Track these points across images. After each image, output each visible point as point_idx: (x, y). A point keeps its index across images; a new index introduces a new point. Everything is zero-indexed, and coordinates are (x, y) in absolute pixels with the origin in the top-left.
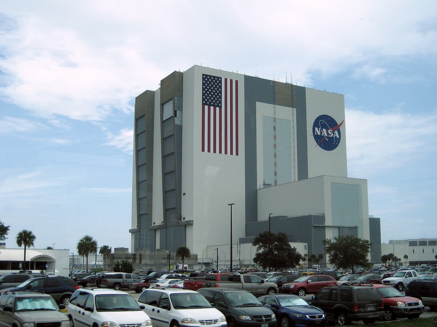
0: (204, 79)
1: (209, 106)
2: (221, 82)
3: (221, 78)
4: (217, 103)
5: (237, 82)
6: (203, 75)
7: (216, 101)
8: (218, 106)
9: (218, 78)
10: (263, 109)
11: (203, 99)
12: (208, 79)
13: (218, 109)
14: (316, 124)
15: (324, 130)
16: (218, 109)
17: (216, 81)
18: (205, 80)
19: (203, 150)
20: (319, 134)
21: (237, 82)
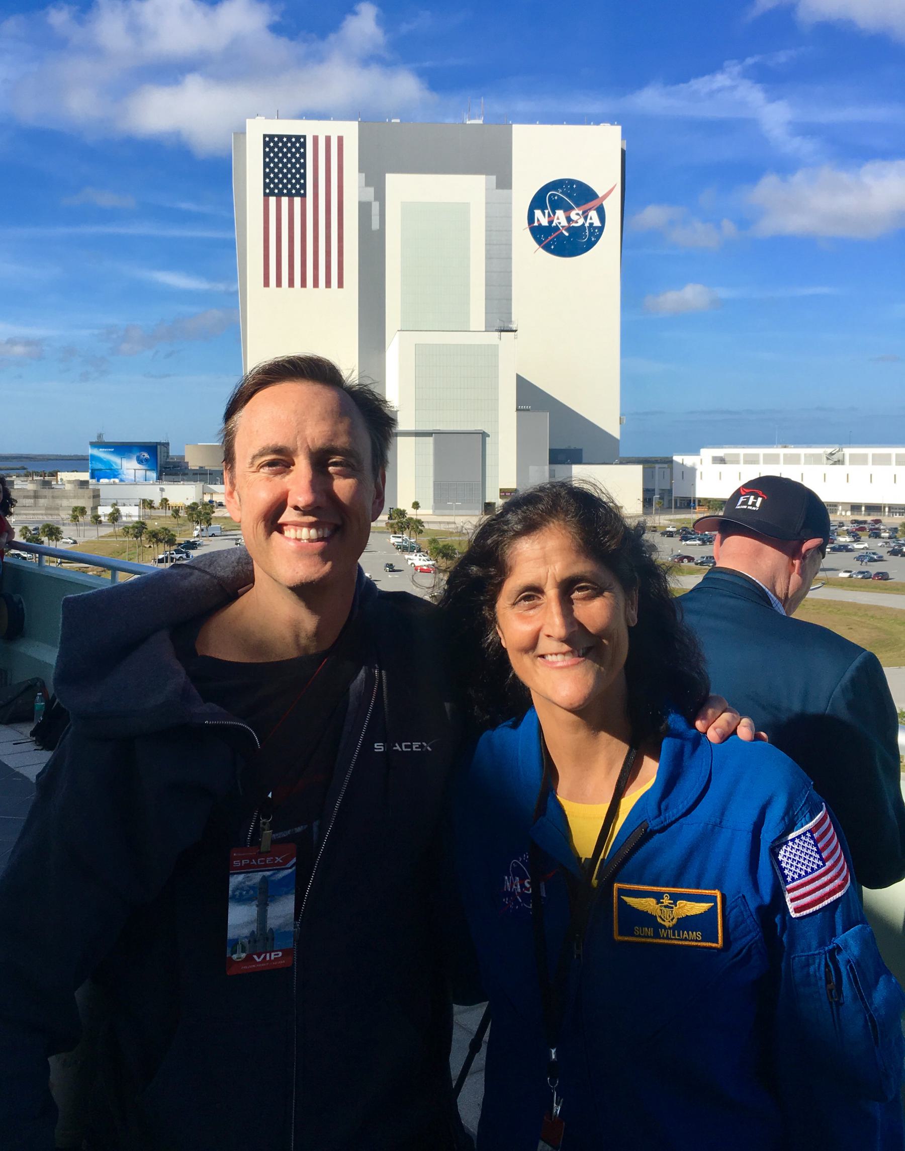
0: (266, 144)
2: (304, 145)
3: (304, 137)
4: (295, 189)
5: (340, 140)
6: (265, 136)
7: (294, 186)
8: (298, 194)
9: (298, 138)
10: (400, 187)
11: (266, 186)
12: (276, 144)
14: (538, 202)
15: (560, 213)
17: (293, 145)
18: (269, 147)
19: (266, 284)
21: (340, 140)
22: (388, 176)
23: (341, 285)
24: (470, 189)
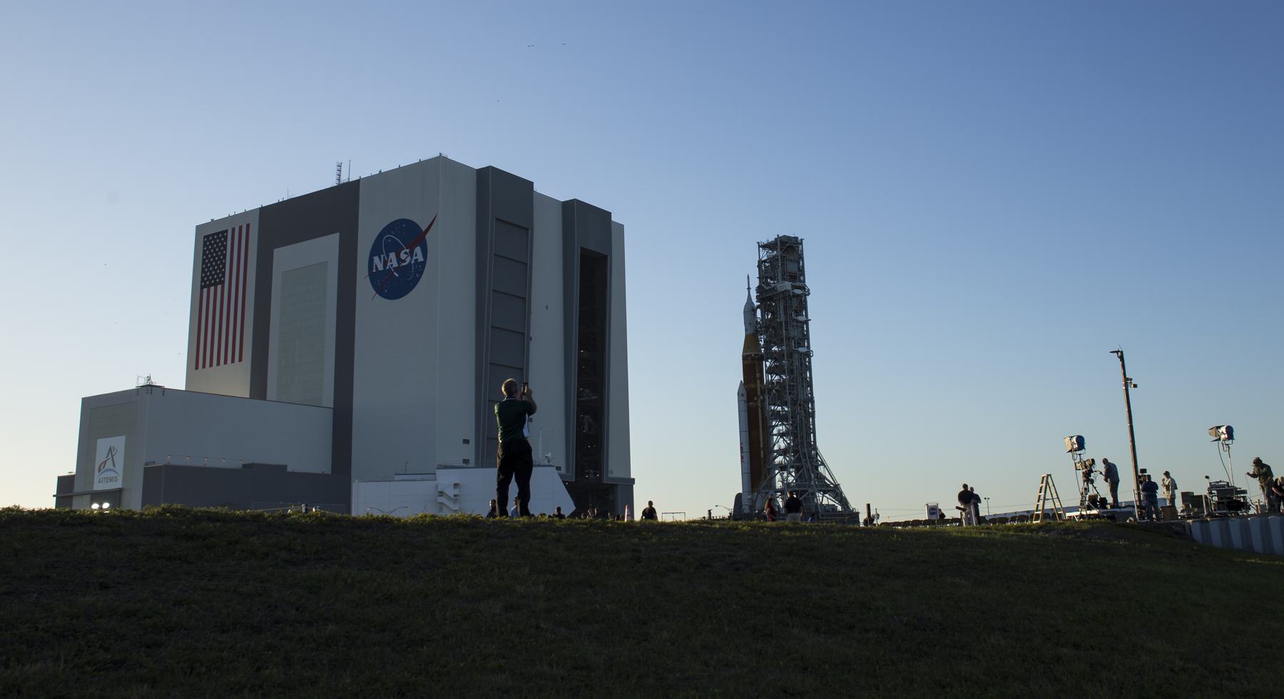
0: (205, 244)
1: (208, 287)
2: (226, 238)
5: (248, 226)
9: (223, 232)
13: (219, 287)
14: (376, 250)
15: (392, 255)
16: (219, 287)
19: (197, 368)
20: (381, 268)
21: (248, 226)
22: (276, 251)
23: (240, 360)
24: (327, 247)
